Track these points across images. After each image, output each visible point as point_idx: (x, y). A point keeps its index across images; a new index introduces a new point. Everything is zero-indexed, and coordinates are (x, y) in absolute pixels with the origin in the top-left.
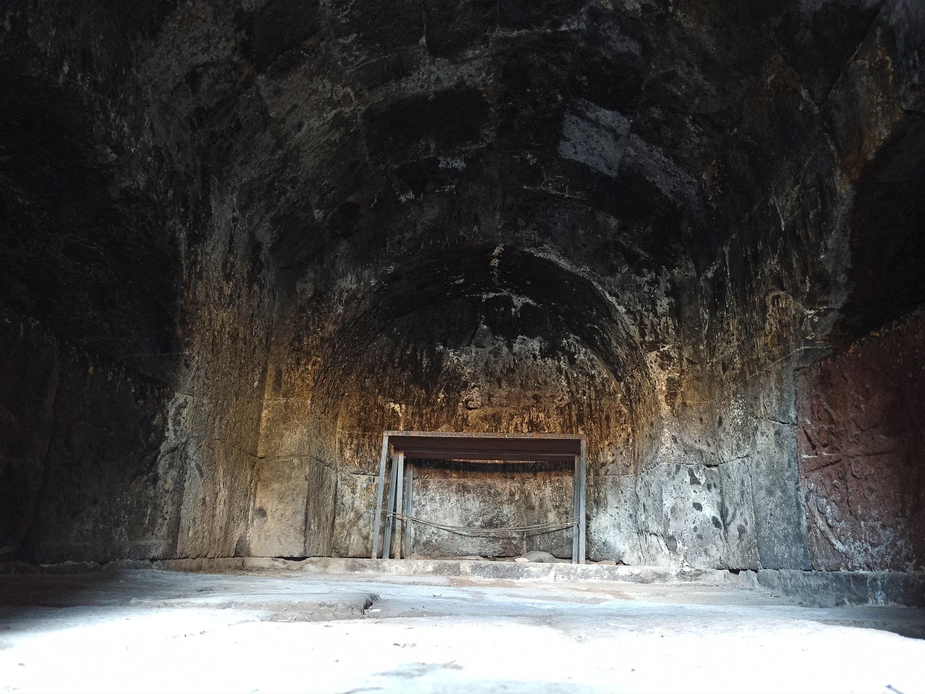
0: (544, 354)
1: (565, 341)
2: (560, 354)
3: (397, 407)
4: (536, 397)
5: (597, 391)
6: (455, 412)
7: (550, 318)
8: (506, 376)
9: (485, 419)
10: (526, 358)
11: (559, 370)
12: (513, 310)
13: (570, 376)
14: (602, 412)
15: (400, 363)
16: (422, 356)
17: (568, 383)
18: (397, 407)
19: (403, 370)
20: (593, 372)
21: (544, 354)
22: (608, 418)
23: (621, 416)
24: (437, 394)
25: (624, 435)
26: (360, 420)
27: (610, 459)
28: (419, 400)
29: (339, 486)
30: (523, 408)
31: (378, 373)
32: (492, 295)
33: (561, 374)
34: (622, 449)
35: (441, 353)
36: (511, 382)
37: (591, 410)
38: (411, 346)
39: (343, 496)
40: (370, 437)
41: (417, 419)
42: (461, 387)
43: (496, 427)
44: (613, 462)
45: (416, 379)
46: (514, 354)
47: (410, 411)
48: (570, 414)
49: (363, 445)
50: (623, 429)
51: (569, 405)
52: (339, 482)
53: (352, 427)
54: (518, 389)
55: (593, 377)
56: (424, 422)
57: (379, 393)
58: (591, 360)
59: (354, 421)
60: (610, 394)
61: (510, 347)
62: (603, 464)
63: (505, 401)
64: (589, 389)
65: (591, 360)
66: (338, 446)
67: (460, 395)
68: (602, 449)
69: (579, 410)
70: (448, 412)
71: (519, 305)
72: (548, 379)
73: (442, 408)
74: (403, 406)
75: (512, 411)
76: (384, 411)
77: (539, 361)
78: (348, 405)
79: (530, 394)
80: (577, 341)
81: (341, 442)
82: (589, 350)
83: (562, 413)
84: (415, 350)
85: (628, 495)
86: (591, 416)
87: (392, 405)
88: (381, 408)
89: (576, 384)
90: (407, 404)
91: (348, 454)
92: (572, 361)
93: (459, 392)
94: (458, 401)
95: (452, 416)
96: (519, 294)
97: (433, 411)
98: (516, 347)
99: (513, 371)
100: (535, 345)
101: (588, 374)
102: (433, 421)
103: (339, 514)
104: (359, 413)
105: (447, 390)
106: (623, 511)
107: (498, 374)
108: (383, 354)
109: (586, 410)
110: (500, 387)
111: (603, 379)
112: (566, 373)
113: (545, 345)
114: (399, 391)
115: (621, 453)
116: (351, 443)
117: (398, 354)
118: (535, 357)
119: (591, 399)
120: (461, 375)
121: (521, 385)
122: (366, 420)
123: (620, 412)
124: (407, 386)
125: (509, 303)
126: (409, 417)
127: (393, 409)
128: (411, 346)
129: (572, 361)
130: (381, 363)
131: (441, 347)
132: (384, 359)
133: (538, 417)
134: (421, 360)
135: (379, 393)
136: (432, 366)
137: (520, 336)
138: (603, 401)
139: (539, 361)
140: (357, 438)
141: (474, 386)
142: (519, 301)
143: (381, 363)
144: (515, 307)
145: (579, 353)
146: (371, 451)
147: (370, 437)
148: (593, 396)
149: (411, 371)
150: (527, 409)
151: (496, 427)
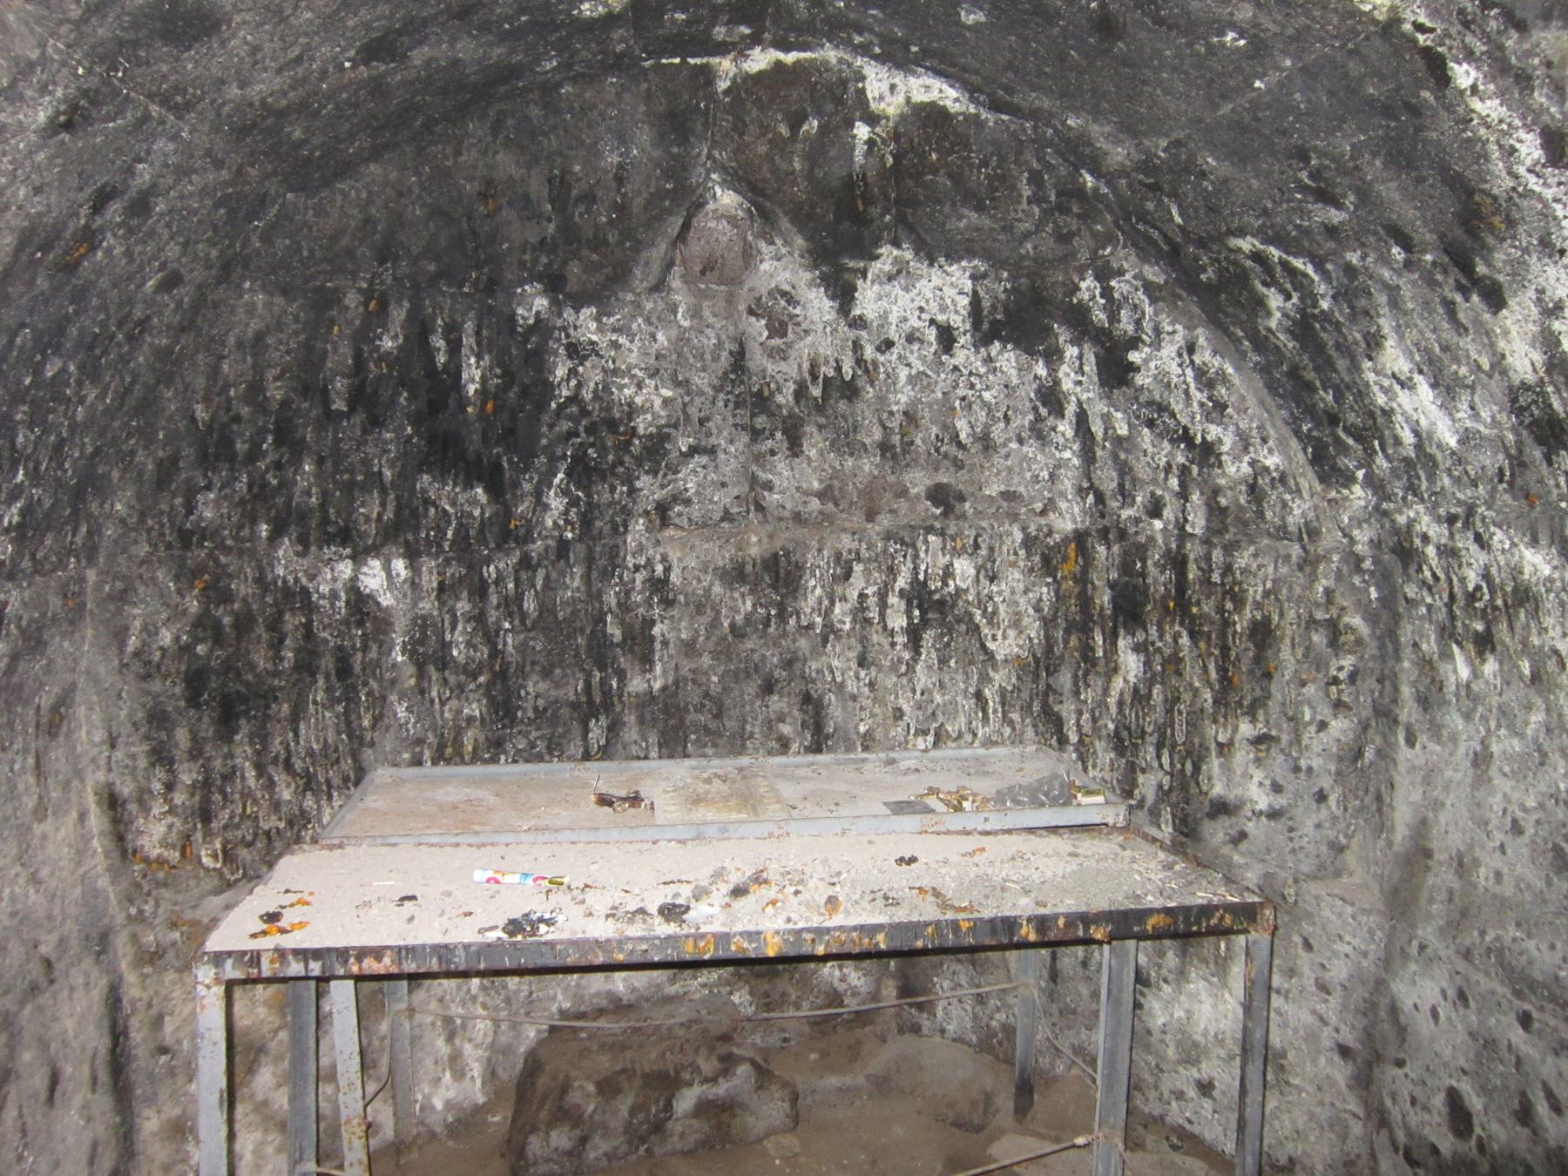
0: (992, 326)
1: (1088, 286)
2: (1063, 334)
3: (373, 578)
4: (939, 495)
5: (1216, 512)
6: (615, 555)
7: (1035, 179)
8: (820, 408)
9: (736, 575)
10: (910, 338)
11: (1051, 398)
12: (862, 131)
13: (1097, 428)
14: (1239, 602)
15: (357, 398)
16: (454, 347)
17: (1088, 456)
18: (373, 578)
19: (375, 422)
20: (1214, 431)
21: (992, 326)
22: (1262, 633)
23: (1334, 643)
24: (538, 494)
25: (1340, 727)
26: (195, 681)
27: (1263, 801)
28: (462, 529)
29: (133, 989)
30: (888, 536)
31: (254, 455)
32: (760, 60)
33: (1060, 413)
34: (1326, 782)
35: (541, 327)
36: (845, 441)
37: (1182, 583)
38: (398, 314)
39: (158, 1022)
40: (261, 737)
41: (463, 606)
42: (639, 461)
43: (781, 608)
44: (1274, 814)
45: (445, 451)
46: (859, 323)
47: (429, 580)
48: (1082, 579)
49: (228, 777)
50: (1338, 705)
51: (1080, 537)
52: (131, 978)
53: (158, 718)
54: (868, 465)
55: (1207, 453)
56: (493, 615)
57: (275, 537)
58: (1206, 379)
59: (171, 690)
60: (1282, 532)
61: (844, 295)
62: (1222, 808)
63: (815, 504)
64: (1184, 495)
65: (1206, 379)
66: (97, 821)
67: (632, 491)
68: (1224, 749)
69: (1126, 567)
70: (590, 560)
71: (892, 107)
72: (998, 432)
73: (563, 547)
74: (399, 565)
75: (846, 543)
76: (309, 608)
77: (963, 355)
78: (120, 635)
79: (918, 481)
80: (1149, 288)
81: (112, 802)
82: (1202, 336)
83: (1048, 567)
84: (419, 331)
85: (1339, 971)
86: (1183, 604)
87: (345, 569)
88: (297, 598)
89: (1124, 470)
90: (412, 556)
91: (155, 833)
92: (1115, 371)
93: (629, 480)
94: (627, 513)
95: (606, 575)
96: (897, 58)
97: (526, 563)
98: (868, 300)
99: (850, 391)
100: (946, 289)
101: (1187, 438)
102: (530, 605)
103: (151, 1099)
104: (186, 650)
105: (583, 473)
106: (1307, 1018)
107: (785, 398)
108: (259, 369)
109: (1159, 579)
110: (795, 448)
111: (1258, 469)
112: (1082, 419)
113: (1000, 287)
114: (371, 510)
115: (1321, 797)
116: (169, 787)
117: (340, 355)
118: (947, 337)
119: (1183, 536)
120: (632, 410)
121: (885, 447)
122: (228, 667)
123: (1334, 629)
124: (406, 476)
125: (843, 100)
126: (428, 606)
127: (353, 587)
128: (398, 314)
129: (1115, 371)
130: (262, 407)
131: (541, 303)
132: (276, 392)
133: (948, 573)
134: (454, 370)
135: (275, 537)
136: (505, 388)
137: (886, 250)
138: (1243, 559)
139: (963, 355)
140: (196, 752)
141: (694, 451)
142: (892, 91)
143: (262, 407)
144: (872, 119)
145: (1157, 344)
146: (271, 785)
147: (261, 737)
148: (1197, 523)
149: (416, 420)
150: (904, 538)
151: (781, 608)
